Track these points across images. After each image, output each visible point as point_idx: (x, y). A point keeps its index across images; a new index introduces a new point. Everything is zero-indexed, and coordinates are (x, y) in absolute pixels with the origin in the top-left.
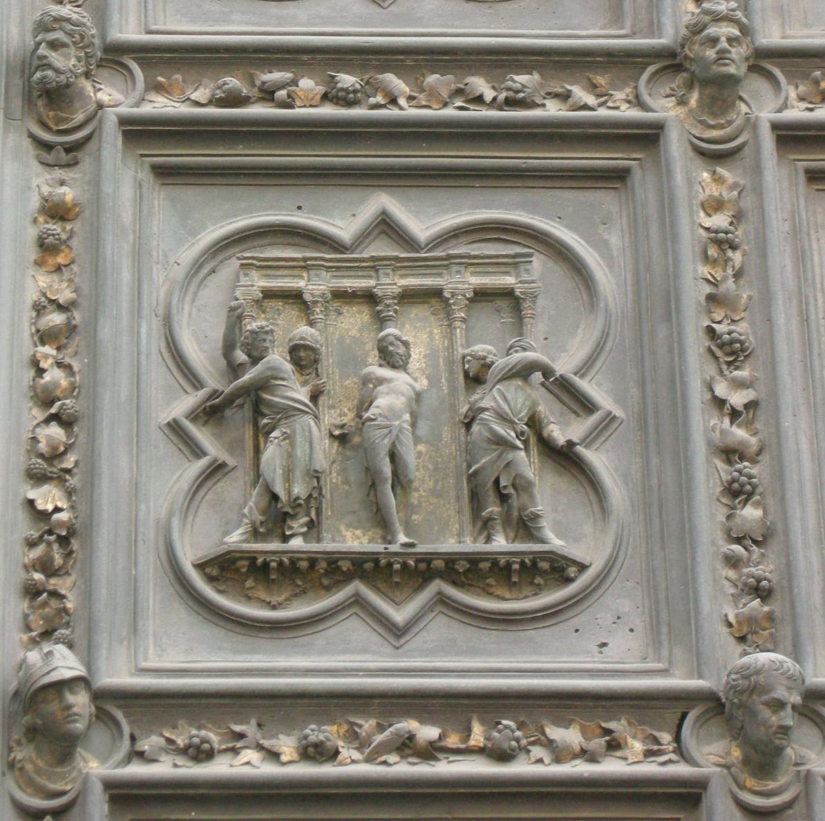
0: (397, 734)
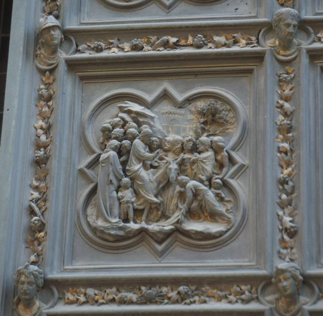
0: (163, 41)
